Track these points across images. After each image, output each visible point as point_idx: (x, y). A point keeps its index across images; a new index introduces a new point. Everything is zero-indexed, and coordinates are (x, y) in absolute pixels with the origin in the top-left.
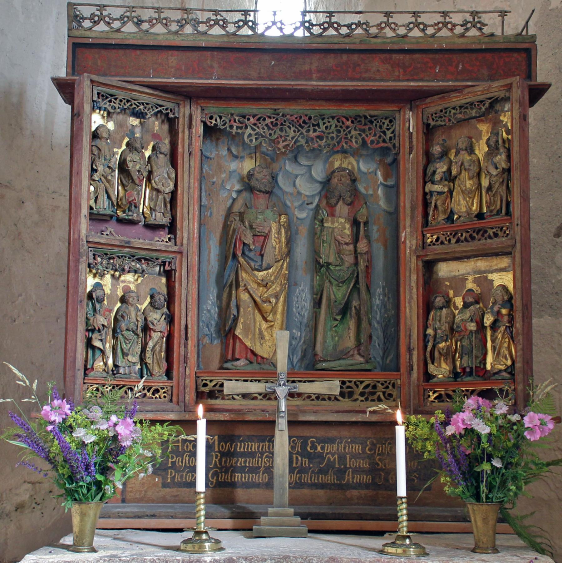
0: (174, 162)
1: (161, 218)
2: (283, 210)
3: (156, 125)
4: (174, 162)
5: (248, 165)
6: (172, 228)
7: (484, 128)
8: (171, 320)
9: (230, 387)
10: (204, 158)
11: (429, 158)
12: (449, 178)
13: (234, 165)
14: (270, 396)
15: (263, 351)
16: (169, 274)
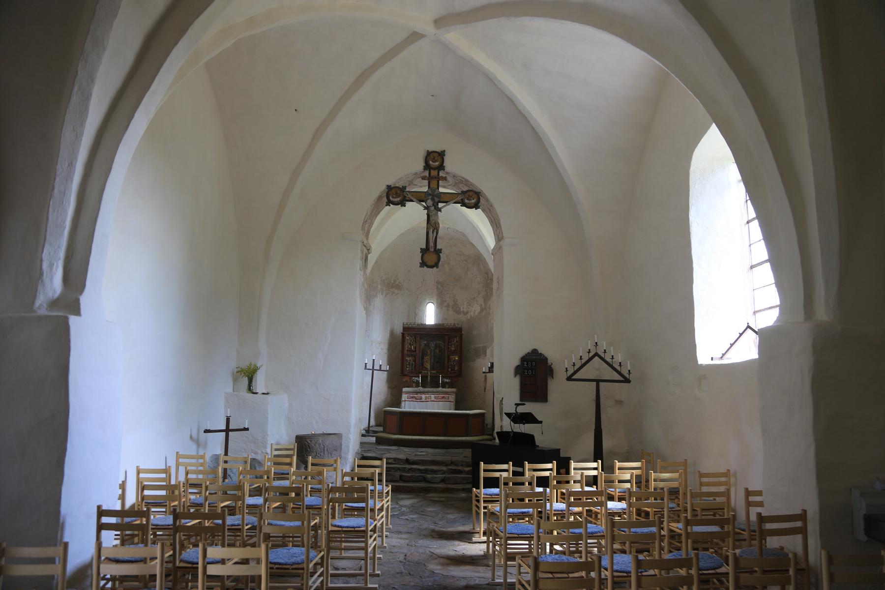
0: (416, 342)
1: (414, 350)
2: (430, 348)
3: (413, 337)
4: (416, 342)
5: (425, 342)
6: (415, 351)
7: (455, 339)
8: (415, 363)
9: (423, 372)
10: (420, 341)
11: (449, 342)
12: (451, 345)
13: (424, 342)
14: (428, 373)
15: (427, 367)
16: (415, 357)
